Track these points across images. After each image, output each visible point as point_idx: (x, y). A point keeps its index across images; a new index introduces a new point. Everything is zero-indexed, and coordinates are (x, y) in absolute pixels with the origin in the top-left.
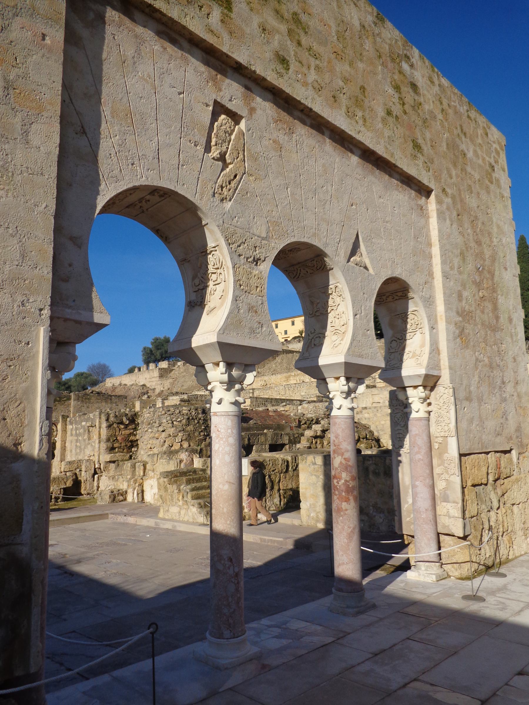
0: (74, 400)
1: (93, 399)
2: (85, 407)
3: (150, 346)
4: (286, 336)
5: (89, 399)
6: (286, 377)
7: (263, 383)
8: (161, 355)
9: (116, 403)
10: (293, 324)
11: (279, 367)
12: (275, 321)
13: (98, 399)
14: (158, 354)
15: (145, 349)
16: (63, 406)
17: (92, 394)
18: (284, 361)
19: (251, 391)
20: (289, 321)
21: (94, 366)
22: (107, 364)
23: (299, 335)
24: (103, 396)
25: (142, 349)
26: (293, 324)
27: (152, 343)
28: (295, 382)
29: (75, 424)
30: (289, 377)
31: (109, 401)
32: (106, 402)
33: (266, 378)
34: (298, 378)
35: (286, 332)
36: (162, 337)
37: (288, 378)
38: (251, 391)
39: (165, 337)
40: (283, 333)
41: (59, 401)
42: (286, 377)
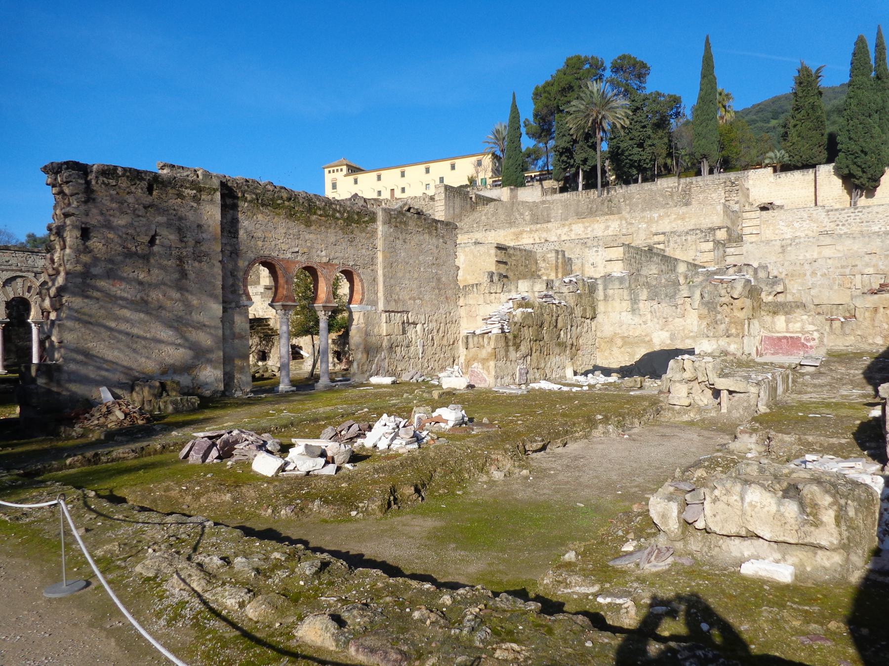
0: (384, 223)
1: (412, 226)
2: (401, 241)
5: (405, 223)
6: (514, 234)
9: (443, 237)
10: (453, 167)
11: (493, 219)
12: (426, 163)
13: (419, 227)
16: (364, 234)
17: (409, 214)
18: (500, 210)
24: (425, 219)
26: (453, 167)
28: (532, 241)
30: (521, 233)
32: (430, 233)
34: (536, 236)
41: (358, 222)
42: (514, 234)
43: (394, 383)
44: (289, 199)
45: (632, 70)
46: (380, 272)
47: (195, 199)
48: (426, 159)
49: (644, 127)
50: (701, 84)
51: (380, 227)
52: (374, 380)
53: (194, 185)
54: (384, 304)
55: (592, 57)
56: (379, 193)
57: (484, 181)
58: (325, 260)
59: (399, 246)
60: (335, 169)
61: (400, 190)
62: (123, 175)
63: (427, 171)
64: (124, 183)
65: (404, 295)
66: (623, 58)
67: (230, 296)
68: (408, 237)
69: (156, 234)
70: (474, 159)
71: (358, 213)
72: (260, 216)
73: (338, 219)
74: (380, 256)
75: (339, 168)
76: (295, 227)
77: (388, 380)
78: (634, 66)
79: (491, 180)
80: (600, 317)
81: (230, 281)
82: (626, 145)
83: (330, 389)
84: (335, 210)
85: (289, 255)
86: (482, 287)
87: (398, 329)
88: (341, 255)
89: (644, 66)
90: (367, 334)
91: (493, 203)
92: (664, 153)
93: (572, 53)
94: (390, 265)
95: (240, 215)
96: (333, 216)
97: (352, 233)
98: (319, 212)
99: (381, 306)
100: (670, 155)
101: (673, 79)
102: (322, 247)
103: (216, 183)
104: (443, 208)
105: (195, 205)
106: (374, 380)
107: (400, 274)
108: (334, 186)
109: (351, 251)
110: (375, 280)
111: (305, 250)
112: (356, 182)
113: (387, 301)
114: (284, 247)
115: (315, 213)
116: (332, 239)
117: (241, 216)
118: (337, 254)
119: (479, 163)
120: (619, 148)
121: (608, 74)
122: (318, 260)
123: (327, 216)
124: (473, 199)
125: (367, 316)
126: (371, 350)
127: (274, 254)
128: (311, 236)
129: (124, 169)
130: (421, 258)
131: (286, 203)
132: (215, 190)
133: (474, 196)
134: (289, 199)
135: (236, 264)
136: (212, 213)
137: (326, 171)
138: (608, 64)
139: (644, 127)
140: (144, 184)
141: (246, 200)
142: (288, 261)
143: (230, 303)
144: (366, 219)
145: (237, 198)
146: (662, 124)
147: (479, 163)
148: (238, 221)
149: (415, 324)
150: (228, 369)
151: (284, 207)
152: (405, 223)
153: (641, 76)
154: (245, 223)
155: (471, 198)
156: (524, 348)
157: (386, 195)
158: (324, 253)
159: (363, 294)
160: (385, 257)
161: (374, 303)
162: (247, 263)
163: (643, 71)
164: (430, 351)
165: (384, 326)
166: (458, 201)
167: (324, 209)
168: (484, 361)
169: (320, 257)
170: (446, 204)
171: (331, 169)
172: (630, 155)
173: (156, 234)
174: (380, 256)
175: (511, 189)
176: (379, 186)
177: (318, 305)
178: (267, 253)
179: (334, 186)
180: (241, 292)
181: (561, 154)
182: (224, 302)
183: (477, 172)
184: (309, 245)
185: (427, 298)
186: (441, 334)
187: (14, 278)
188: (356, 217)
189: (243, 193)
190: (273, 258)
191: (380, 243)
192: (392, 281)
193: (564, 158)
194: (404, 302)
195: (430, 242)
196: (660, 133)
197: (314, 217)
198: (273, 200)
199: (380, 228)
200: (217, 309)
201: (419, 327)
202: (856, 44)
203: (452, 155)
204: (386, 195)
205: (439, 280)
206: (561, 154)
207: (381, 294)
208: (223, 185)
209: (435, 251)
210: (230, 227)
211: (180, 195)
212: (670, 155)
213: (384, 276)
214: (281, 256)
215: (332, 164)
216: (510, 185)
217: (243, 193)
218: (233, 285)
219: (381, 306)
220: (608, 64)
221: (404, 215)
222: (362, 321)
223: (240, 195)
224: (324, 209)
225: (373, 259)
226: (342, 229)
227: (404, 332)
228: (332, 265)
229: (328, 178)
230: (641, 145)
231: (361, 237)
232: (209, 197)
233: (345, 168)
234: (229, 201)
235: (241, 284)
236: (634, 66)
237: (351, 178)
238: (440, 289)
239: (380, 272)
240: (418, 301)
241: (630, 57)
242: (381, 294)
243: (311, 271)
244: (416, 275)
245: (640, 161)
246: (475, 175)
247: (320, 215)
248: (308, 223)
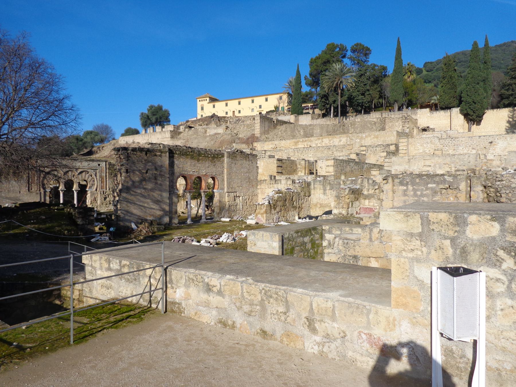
0: (227, 158)
3: (146, 112)
4: (260, 110)
6: (294, 142)
7: (273, 146)
8: (157, 119)
10: (267, 100)
11: (284, 134)
12: (252, 97)
14: (153, 119)
15: (142, 114)
18: (288, 129)
19: (264, 152)
20: (264, 98)
21: (98, 126)
22: (110, 124)
23: (274, 109)
26: (267, 100)
27: (148, 110)
28: (303, 146)
29: (413, 185)
30: (298, 142)
32: (246, 160)
33: (276, 142)
34: (305, 144)
35: (260, 107)
37: (296, 143)
38: (264, 152)
39: (159, 106)
40: (258, 107)
41: (217, 158)
42: (294, 142)
43: (230, 221)
44: (192, 152)
45: (362, 51)
46: (225, 177)
47: (160, 156)
49: (365, 85)
50: (395, 63)
51: (226, 159)
52: (223, 219)
53: (160, 151)
55: (341, 44)
56: (227, 113)
57: (283, 108)
58: (204, 174)
59: (233, 166)
60: (203, 99)
61: (238, 112)
63: (253, 101)
64: (139, 153)
65: (235, 185)
66: (357, 45)
67: (171, 189)
68: (237, 162)
70: (278, 96)
71: (217, 154)
72: (181, 159)
74: (225, 170)
75: (205, 99)
76: (194, 162)
77: (228, 220)
78: (363, 49)
79: (287, 108)
80: (312, 196)
81: (171, 184)
82: (355, 94)
83: (206, 223)
84: (208, 154)
85: (191, 173)
86: (267, 182)
87: (232, 199)
89: (368, 49)
91: (284, 125)
92: (378, 96)
93: (330, 42)
94: (229, 174)
98: (203, 156)
99: (226, 190)
100: (381, 97)
101: (382, 58)
103: (167, 149)
104: (259, 127)
106: (223, 219)
107: (233, 177)
108: (202, 109)
109: (214, 169)
112: (214, 106)
113: (228, 188)
114: (190, 170)
116: (207, 166)
117: (175, 160)
119: (281, 98)
120: (352, 95)
121: (349, 53)
123: (205, 157)
125: (220, 195)
126: (222, 208)
128: (200, 165)
130: (242, 170)
132: (166, 152)
134: (192, 152)
136: (165, 160)
137: (198, 100)
138: (349, 48)
139: (365, 85)
141: (176, 154)
146: (376, 81)
147: (281, 98)
149: (239, 197)
151: (190, 155)
152: (236, 157)
153: (366, 55)
154: (176, 162)
156: (278, 209)
157: (230, 114)
160: (227, 171)
161: (223, 189)
163: (368, 52)
164: (245, 207)
165: (227, 198)
166: (267, 124)
167: (204, 154)
168: (262, 214)
170: (260, 125)
171: (201, 99)
172: (357, 100)
174: (225, 170)
176: (227, 109)
177: (202, 191)
179: (202, 109)
181: (322, 98)
183: (279, 103)
185: (244, 186)
186: (250, 201)
187: (68, 172)
191: (225, 165)
193: (323, 100)
194: (235, 188)
195: (246, 163)
196: (376, 86)
198: (186, 153)
201: (241, 198)
202: (473, 45)
203: (266, 94)
204: (230, 114)
205: (249, 178)
206: (322, 98)
207: (225, 186)
208: (169, 149)
210: (172, 164)
212: (381, 97)
213: (227, 178)
215: (201, 96)
216: (295, 113)
219: (226, 190)
220: (349, 48)
221: (235, 153)
224: (204, 154)
225: (223, 172)
227: (235, 200)
229: (199, 104)
230: (363, 94)
231: (218, 164)
233: (208, 99)
234: (171, 155)
236: (363, 49)
237: (211, 105)
238: (250, 182)
239: (225, 177)
240: (241, 188)
241: (361, 44)
242: (225, 186)
243: (199, 178)
244: (240, 177)
245: (363, 102)
246: (278, 105)
248: (198, 160)
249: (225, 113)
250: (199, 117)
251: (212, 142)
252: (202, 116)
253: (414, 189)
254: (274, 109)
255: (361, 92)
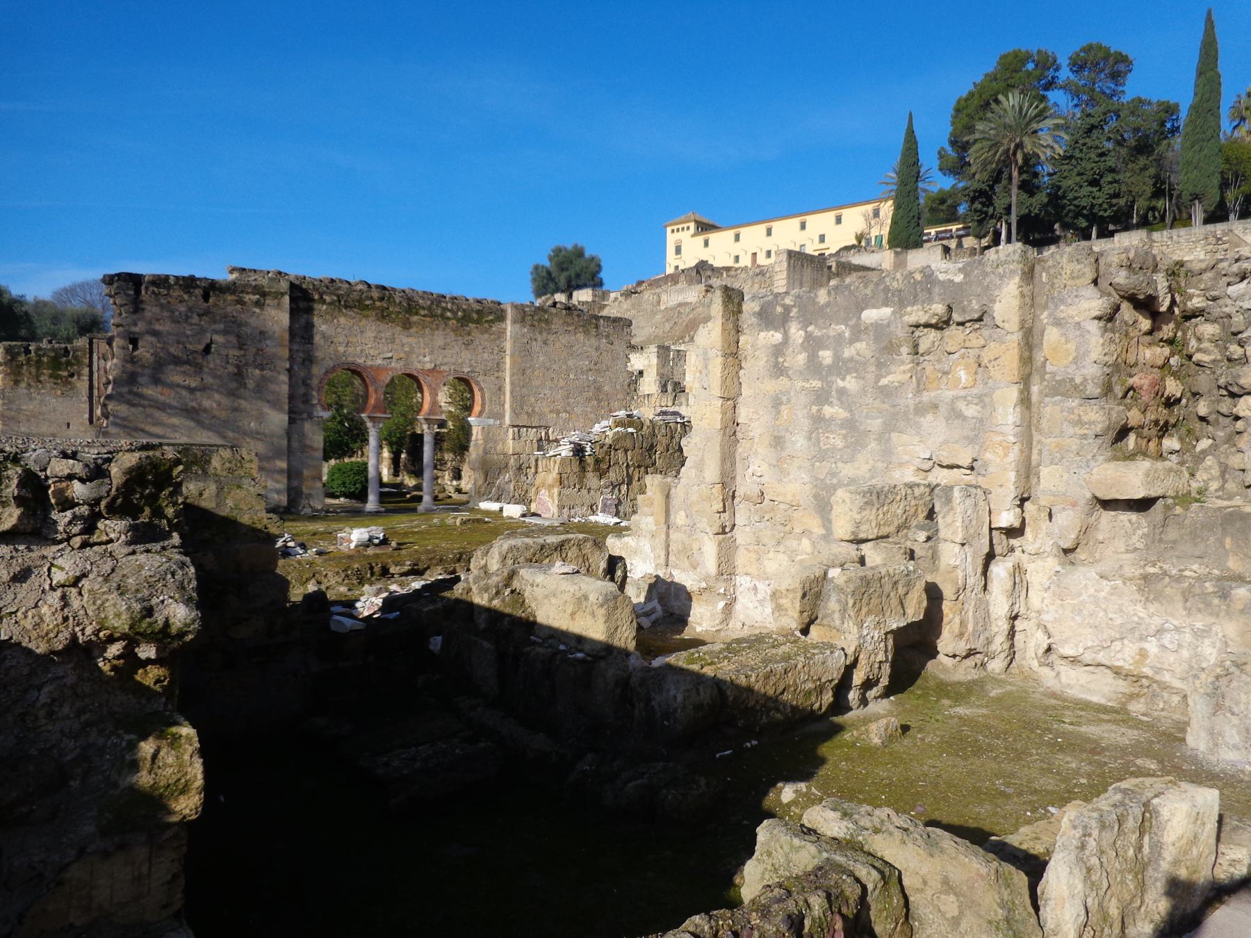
0: (514, 322)
1: (557, 324)
2: (540, 343)
3: (547, 264)
4: (822, 246)
5: (547, 322)
9: (607, 336)
10: (839, 220)
12: (801, 215)
13: (568, 325)
15: (536, 268)
16: (486, 336)
17: (553, 310)
23: (855, 242)
24: (579, 316)
25: (530, 269)
26: (839, 220)
27: (551, 259)
29: (805, 323)
31: (593, 331)
32: (587, 332)
35: (822, 239)
36: (570, 246)
39: (576, 246)
40: (817, 239)
41: (478, 322)
44: (381, 299)
45: (1103, 65)
47: (258, 304)
48: (766, 216)
49: (1102, 155)
50: (1196, 86)
51: (509, 327)
53: (258, 290)
54: (511, 418)
55: (1039, 52)
56: (737, 259)
57: (879, 238)
58: (429, 366)
60: (680, 226)
61: (764, 254)
62: (176, 284)
63: (803, 226)
64: (176, 293)
66: (1088, 49)
67: (301, 406)
68: (551, 337)
69: (211, 342)
70: (870, 208)
72: (342, 320)
73: (448, 319)
75: (685, 226)
78: (1106, 59)
81: (302, 390)
82: (1070, 182)
84: (445, 309)
85: (379, 362)
86: (653, 399)
88: (453, 360)
89: (1123, 59)
90: (486, 452)
92: (1149, 190)
93: (1009, 49)
94: (521, 371)
95: (315, 319)
96: (442, 316)
97: (469, 334)
98: (422, 312)
99: (507, 420)
100: (1158, 193)
101: (1160, 77)
102: (425, 351)
103: (284, 286)
104: (784, 282)
105: (257, 310)
107: (536, 383)
108: (678, 250)
109: (466, 355)
110: (500, 388)
111: (402, 355)
112: (706, 244)
113: (515, 413)
114: (372, 352)
115: (417, 314)
117: (316, 320)
118: (446, 360)
119: (876, 213)
120: (1059, 188)
121: (1065, 74)
122: (419, 366)
123: (432, 316)
124: (833, 269)
125: (486, 431)
127: (360, 361)
128: (410, 340)
129: (177, 278)
130: (570, 363)
131: (378, 304)
132: (283, 294)
133: (834, 265)
134: (381, 299)
135: (309, 370)
136: (278, 317)
137: (669, 229)
138: (1064, 61)
139: (1102, 155)
140: (198, 292)
141: (324, 302)
142: (378, 368)
143: (301, 413)
144: (491, 317)
145: (313, 300)
146: (1143, 147)
147: (876, 213)
148: (312, 326)
150: (295, 483)
151: (374, 308)
152: (547, 322)
153: (1116, 76)
155: (830, 267)
156: (613, 475)
157: (745, 261)
158: (427, 359)
159: (483, 405)
161: (500, 416)
162: (323, 371)
163: (1122, 67)
165: (510, 442)
166: (808, 273)
168: (551, 487)
169: (423, 362)
170: (788, 277)
171: (675, 227)
172: (1075, 198)
173: (211, 342)
174: (508, 360)
175: (896, 253)
176: (737, 249)
178: (350, 359)
179: (678, 250)
180: (315, 402)
181: (973, 200)
182: (291, 412)
183: (870, 227)
184: (407, 349)
185: (578, 410)
188: (475, 316)
189: (321, 296)
190: (358, 365)
191: (508, 346)
192: (524, 391)
193: (977, 206)
195: (585, 343)
196: (1142, 160)
197: (415, 318)
198: (359, 301)
199: (509, 328)
200: (277, 419)
203: (836, 203)
204: (745, 261)
205: (599, 389)
206: (973, 200)
208: (292, 285)
209: (594, 354)
210: (302, 332)
211: (240, 302)
212: (1158, 193)
213: (512, 383)
214: (369, 363)
215: (677, 220)
216: (897, 246)
217: (321, 296)
218: (305, 395)
219: (507, 420)
220: (1064, 61)
222: (480, 437)
223: (316, 297)
224: (429, 308)
225: (499, 366)
226: (454, 331)
228: (440, 372)
229: (671, 239)
230: (1094, 183)
231: (481, 339)
232: (276, 302)
233: (692, 225)
234: (302, 305)
235: (314, 393)
236: (1106, 59)
237: (700, 239)
238: (599, 401)
240: (564, 415)
241: (1100, 47)
242: (507, 406)
244: (562, 383)
245: (1093, 206)
247: (425, 316)
248: (407, 325)
249: (732, 259)
250: (670, 270)
251: (668, 326)
252: (677, 267)
253: (809, 336)
254: (855, 242)
255: (1089, 175)
